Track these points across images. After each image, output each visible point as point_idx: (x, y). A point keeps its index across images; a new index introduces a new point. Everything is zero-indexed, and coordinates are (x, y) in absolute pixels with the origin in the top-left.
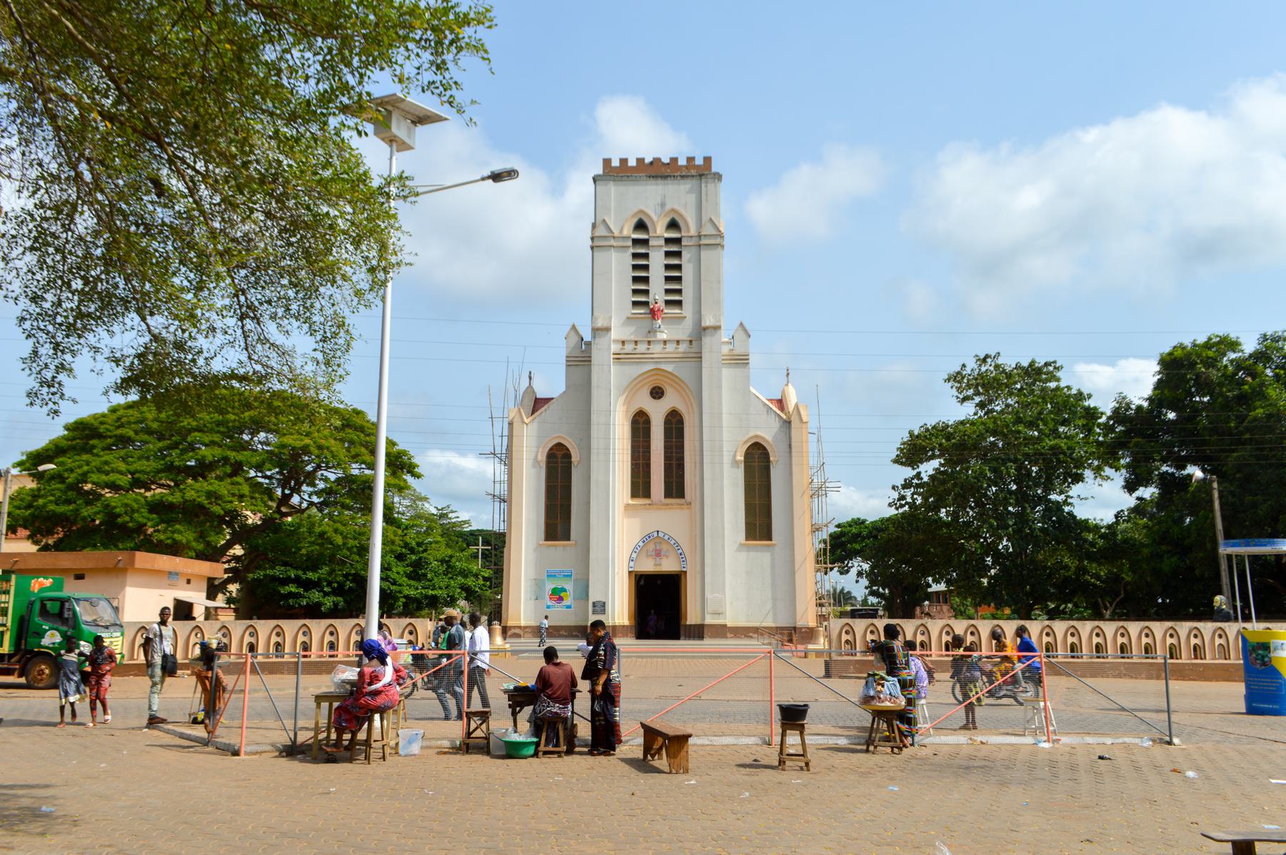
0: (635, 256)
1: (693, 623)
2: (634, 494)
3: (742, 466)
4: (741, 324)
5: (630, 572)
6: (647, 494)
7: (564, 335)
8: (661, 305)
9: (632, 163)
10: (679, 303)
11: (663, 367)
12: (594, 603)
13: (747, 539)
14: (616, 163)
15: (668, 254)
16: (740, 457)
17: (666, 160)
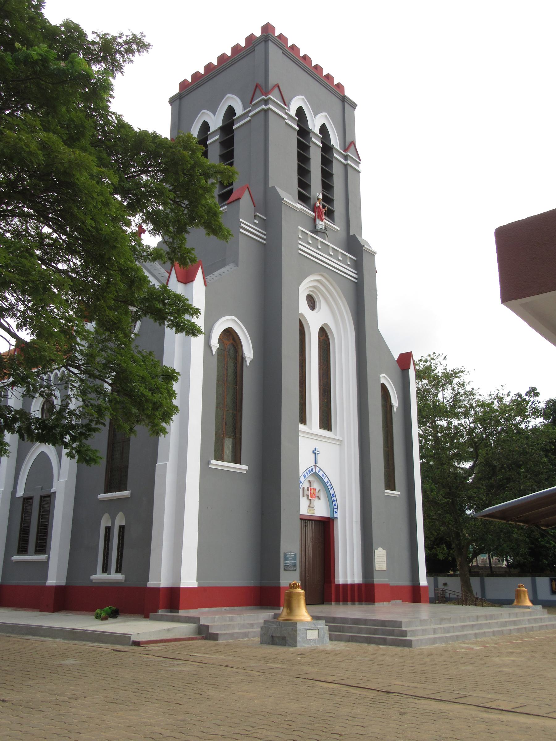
1: (349, 582)
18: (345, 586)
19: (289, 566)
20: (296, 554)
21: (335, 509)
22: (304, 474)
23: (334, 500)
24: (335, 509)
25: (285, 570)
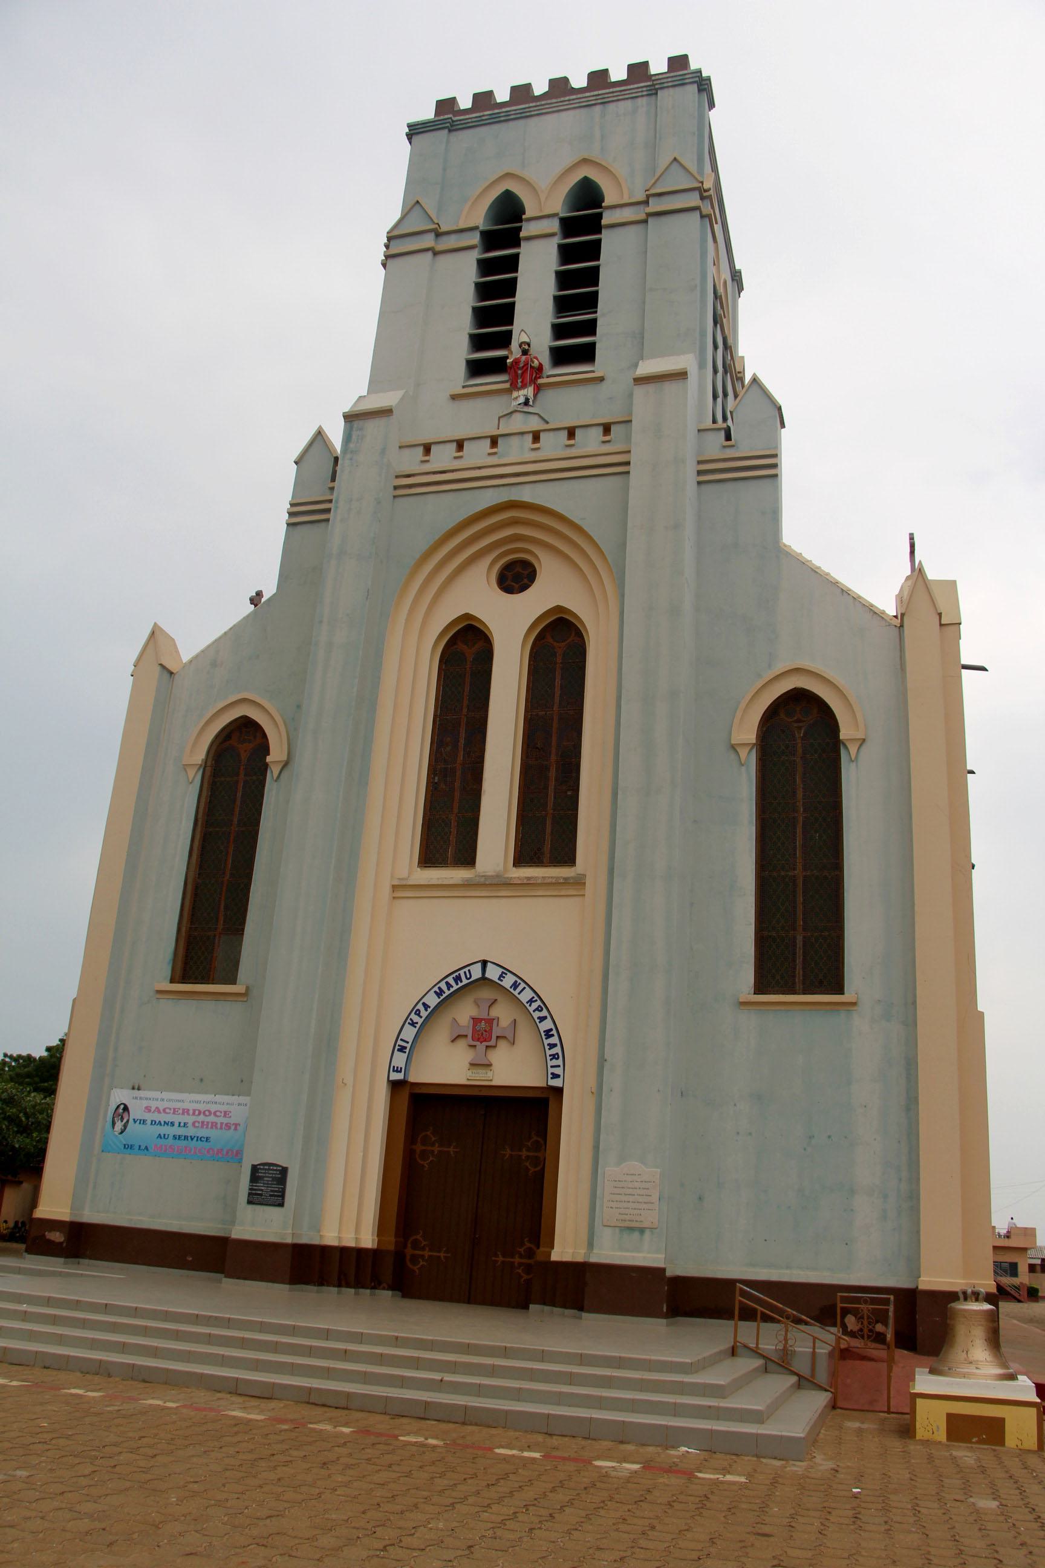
1: (567, 1258)
2: (429, 857)
3: (751, 760)
5: (396, 1086)
6: (467, 857)
7: (295, 455)
10: (587, 354)
11: (526, 495)
12: (255, 1169)
13: (759, 988)
15: (567, 253)
16: (748, 732)
17: (579, 81)
19: (261, 1195)
20: (284, 1171)
21: (552, 1067)
22: (436, 989)
24: (552, 1067)
25: (250, 1202)
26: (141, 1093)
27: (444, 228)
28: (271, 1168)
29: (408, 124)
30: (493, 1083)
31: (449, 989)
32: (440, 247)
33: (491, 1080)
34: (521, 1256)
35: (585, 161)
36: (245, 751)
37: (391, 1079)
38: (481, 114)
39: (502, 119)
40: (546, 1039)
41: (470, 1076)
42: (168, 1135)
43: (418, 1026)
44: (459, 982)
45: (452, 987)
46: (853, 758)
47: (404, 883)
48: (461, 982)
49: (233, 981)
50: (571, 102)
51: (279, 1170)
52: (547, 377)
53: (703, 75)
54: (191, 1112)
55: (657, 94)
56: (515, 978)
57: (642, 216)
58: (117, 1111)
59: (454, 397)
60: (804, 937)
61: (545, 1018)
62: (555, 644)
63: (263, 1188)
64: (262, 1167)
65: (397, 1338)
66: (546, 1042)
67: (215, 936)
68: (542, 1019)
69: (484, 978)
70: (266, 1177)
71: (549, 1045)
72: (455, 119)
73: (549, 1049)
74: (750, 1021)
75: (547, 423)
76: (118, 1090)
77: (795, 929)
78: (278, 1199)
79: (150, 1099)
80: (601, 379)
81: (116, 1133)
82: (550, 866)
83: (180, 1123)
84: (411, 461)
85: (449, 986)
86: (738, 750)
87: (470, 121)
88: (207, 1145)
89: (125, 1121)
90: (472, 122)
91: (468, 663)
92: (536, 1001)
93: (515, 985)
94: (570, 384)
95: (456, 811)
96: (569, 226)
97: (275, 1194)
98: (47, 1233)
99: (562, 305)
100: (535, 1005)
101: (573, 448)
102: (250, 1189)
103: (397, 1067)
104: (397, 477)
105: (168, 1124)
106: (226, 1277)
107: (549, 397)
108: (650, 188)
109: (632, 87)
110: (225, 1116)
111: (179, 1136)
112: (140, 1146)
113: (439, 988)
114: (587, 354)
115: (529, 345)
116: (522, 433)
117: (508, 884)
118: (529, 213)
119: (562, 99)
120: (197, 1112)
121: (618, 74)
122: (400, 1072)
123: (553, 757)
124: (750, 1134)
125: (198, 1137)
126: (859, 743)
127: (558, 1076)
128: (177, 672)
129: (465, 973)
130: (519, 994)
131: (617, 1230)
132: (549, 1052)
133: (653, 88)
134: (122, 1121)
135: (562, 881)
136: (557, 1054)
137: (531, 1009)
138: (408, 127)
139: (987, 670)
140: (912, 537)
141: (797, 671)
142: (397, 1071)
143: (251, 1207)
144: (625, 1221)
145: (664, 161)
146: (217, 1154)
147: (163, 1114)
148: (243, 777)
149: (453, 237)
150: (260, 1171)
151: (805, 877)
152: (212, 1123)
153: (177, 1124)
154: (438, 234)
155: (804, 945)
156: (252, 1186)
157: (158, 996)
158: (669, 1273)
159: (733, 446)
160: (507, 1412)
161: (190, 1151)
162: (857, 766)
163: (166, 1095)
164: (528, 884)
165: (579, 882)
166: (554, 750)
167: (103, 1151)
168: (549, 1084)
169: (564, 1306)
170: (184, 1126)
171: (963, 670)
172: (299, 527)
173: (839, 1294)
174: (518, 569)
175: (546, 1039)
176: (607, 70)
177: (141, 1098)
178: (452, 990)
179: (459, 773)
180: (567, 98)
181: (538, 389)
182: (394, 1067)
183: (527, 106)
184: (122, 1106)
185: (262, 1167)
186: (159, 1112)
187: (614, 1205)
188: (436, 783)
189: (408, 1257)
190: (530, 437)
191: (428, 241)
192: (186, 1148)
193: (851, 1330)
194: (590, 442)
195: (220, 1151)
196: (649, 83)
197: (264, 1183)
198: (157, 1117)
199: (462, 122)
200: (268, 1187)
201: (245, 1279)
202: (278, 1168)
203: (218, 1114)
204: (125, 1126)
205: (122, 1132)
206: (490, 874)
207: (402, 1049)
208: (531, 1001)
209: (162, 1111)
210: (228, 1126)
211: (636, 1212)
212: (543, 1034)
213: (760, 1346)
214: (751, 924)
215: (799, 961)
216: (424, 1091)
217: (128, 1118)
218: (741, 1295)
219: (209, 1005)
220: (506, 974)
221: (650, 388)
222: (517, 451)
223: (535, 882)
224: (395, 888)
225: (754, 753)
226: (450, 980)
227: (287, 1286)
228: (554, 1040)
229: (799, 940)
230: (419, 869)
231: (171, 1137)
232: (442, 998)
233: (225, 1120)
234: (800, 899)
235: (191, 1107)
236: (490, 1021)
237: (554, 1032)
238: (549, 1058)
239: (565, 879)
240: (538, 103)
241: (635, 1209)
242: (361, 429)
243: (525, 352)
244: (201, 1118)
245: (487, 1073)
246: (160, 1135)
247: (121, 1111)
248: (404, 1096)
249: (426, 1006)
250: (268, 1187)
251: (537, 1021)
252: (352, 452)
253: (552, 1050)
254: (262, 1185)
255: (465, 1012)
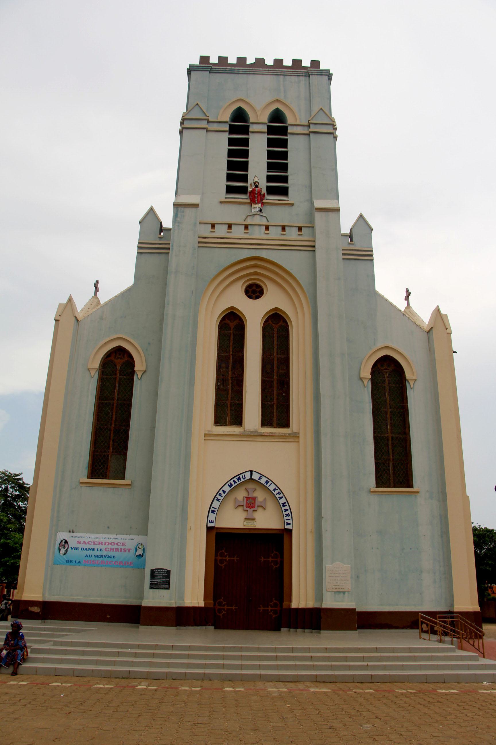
0: (231, 142)
1: (302, 605)
2: (219, 421)
4: (361, 216)
5: (209, 529)
6: (238, 421)
7: (139, 219)
8: (264, 191)
9: (232, 60)
10: (284, 191)
11: (264, 254)
12: (152, 572)
13: (378, 485)
14: (214, 60)
15: (270, 143)
16: (367, 374)
17: (269, 62)
18: (297, 610)
20: (169, 572)
21: (286, 520)
22: (229, 483)
23: (286, 510)
24: (286, 520)
25: (151, 588)
26: (74, 534)
27: (211, 119)
28: (162, 571)
29: (190, 65)
30: (257, 527)
31: (235, 484)
32: (209, 129)
33: (255, 526)
34: (272, 607)
35: (278, 101)
36: (119, 363)
37: (208, 526)
38: (226, 68)
39: (236, 72)
40: (283, 507)
41: (245, 524)
42: (91, 555)
43: (221, 501)
44: (240, 480)
45: (236, 483)
46: (412, 387)
47: (210, 433)
48: (241, 480)
49: (123, 478)
50: (269, 71)
51: (165, 572)
52: (267, 200)
53: (330, 73)
54: (104, 543)
55: (309, 76)
56: (267, 479)
57: (307, 132)
58: (61, 543)
59: (221, 202)
60: (393, 463)
61: (282, 497)
62: (274, 325)
63: (158, 581)
64: (156, 570)
65: (326, 648)
66: (283, 508)
67: (108, 456)
68: (281, 498)
69: (251, 479)
70: (159, 575)
71: (284, 510)
72: (213, 67)
73: (285, 512)
74: (374, 499)
75: (268, 221)
76: (61, 533)
77: (389, 460)
78: (166, 585)
79: (80, 537)
80: (292, 205)
81: (62, 555)
82: (277, 427)
83: (98, 549)
84: (206, 231)
85: (235, 482)
86: (364, 381)
87: (220, 70)
88: (114, 560)
89: (66, 548)
90: (221, 71)
91: (231, 329)
92: (277, 489)
93: (267, 482)
94: (282, 205)
95: (230, 399)
96: (271, 130)
97: (165, 583)
98: (29, 608)
99: (270, 167)
100: (277, 492)
101: (285, 235)
102: (151, 581)
103: (211, 521)
104: (199, 237)
105: (91, 550)
106: (141, 625)
107: (268, 211)
108: (311, 120)
109: (298, 71)
110: (94, 544)
111: (98, 555)
112: (76, 561)
113: (230, 483)
114: (284, 191)
115: (258, 183)
116: (260, 225)
117: (262, 435)
118: (252, 120)
119: (265, 69)
120: (107, 544)
121: (288, 62)
122: (213, 522)
123: (276, 377)
124: (378, 548)
125: (108, 556)
126: (414, 381)
127: (289, 524)
128: (80, 321)
129: (242, 476)
130: (269, 486)
131: (333, 593)
132: (285, 513)
133: (308, 73)
134: (64, 549)
135: (287, 435)
136: (289, 514)
137: (275, 493)
138: (189, 66)
139: (457, 353)
140: (407, 290)
141: (387, 347)
142: (211, 522)
143: (151, 590)
144: (337, 588)
145: (315, 109)
146: (120, 564)
147: (88, 545)
148: (118, 376)
149: (215, 124)
150: (155, 572)
151: (392, 437)
152: (116, 549)
153: (96, 550)
154: (208, 122)
155: (393, 466)
156: (151, 580)
157: (81, 485)
158: (357, 610)
159: (353, 244)
160: (408, 675)
161: (104, 563)
162: (413, 391)
163: (88, 535)
164: (271, 436)
165: (295, 436)
166: (275, 374)
167: (54, 564)
168: (285, 528)
169: (304, 628)
170: (100, 550)
171: (454, 353)
172: (144, 254)
173: (437, 615)
174: (254, 288)
175: (283, 507)
176: (283, 59)
177: (74, 537)
178: (236, 484)
179: (230, 381)
180: (267, 69)
181: (263, 204)
182: (209, 520)
183: (248, 68)
184: (64, 541)
185: (156, 570)
186: (85, 543)
187: (331, 581)
188: (219, 386)
189: (217, 610)
190: (264, 228)
191: (204, 124)
192: (102, 561)
193: (425, 630)
194: (292, 234)
195: (121, 563)
196: (306, 71)
197: (158, 578)
198: (85, 546)
199: (216, 69)
200: (160, 580)
201: (152, 625)
202: (165, 571)
203: (119, 544)
204: (67, 551)
205: (65, 554)
206: (252, 430)
207: (213, 512)
208: (275, 490)
209: (87, 543)
210: (125, 550)
211: (342, 584)
212: (281, 505)
213: (430, 639)
214: (373, 457)
215: (391, 473)
216: (222, 531)
217: (68, 547)
218: (421, 618)
219: (110, 490)
220: (262, 477)
221: (323, 214)
222: (258, 233)
223: (275, 435)
224: (205, 434)
225: (370, 381)
226: (235, 479)
227: (175, 628)
228: (287, 507)
229: (391, 464)
230: (214, 426)
231: (93, 556)
232: (232, 488)
233: (123, 547)
234: (391, 447)
235: (104, 541)
236: (254, 499)
237: (287, 504)
238: (285, 516)
239: (289, 434)
240: (254, 69)
241: (341, 583)
242: (183, 212)
243: (257, 186)
244: (110, 546)
245: (253, 523)
246: (86, 555)
247: (63, 543)
248: (213, 534)
249: (224, 492)
250: (160, 580)
251: (278, 499)
252: (179, 222)
253: (286, 512)
254: (157, 579)
255: (241, 495)
